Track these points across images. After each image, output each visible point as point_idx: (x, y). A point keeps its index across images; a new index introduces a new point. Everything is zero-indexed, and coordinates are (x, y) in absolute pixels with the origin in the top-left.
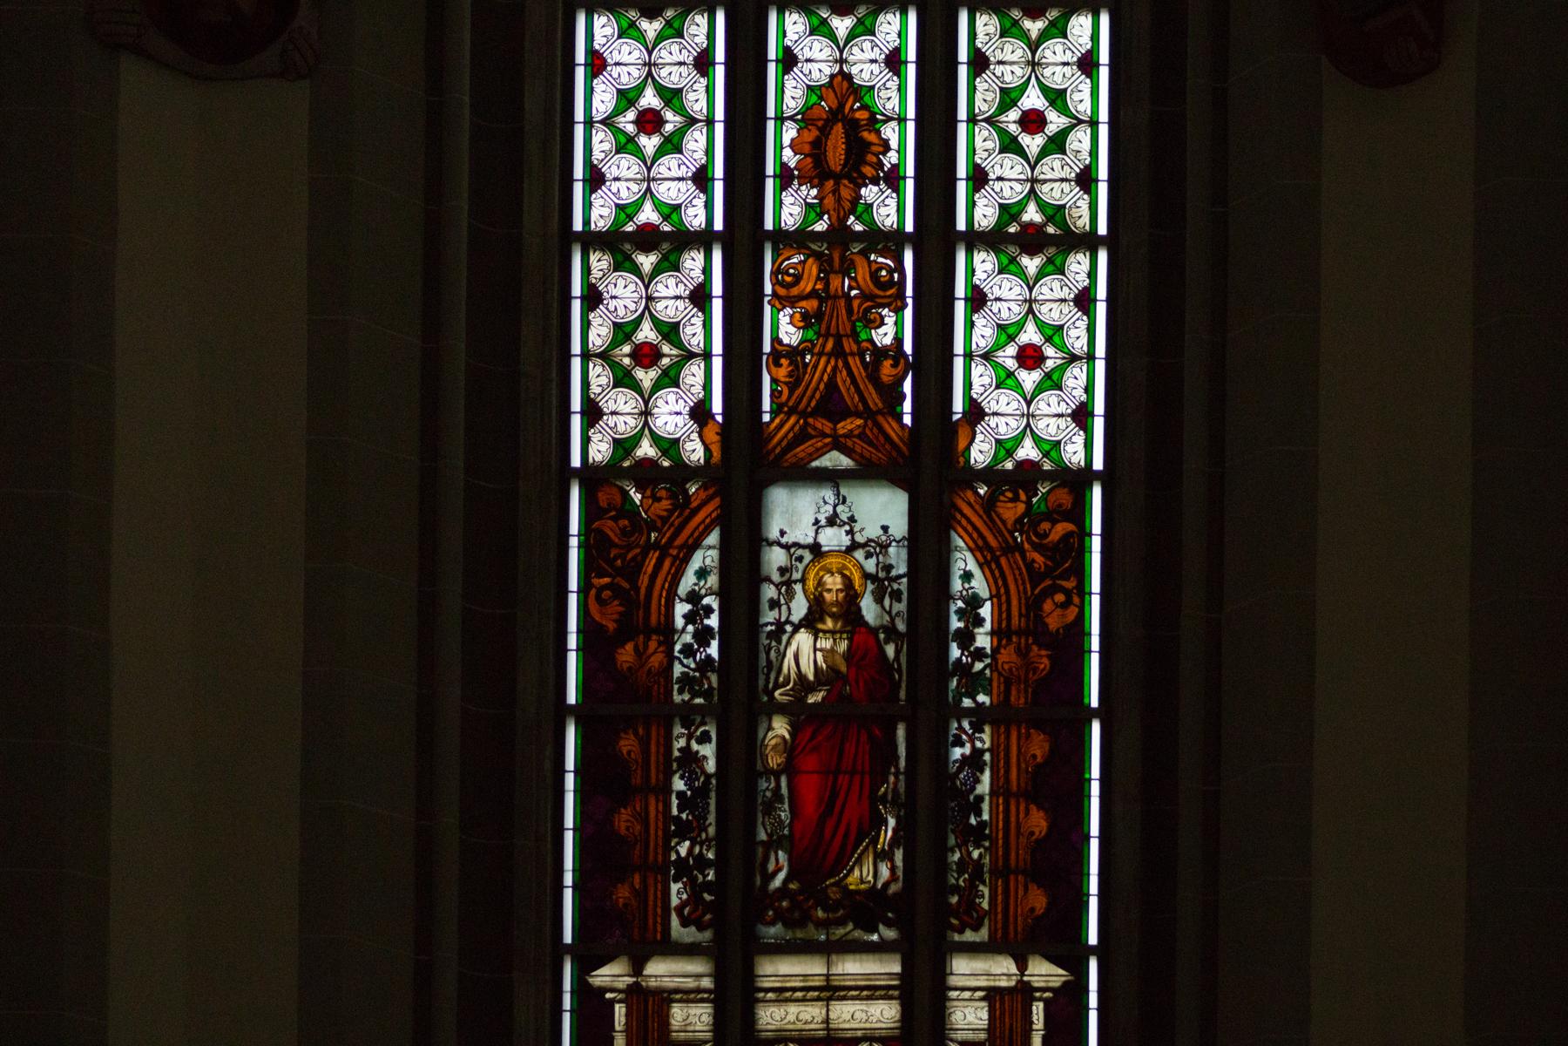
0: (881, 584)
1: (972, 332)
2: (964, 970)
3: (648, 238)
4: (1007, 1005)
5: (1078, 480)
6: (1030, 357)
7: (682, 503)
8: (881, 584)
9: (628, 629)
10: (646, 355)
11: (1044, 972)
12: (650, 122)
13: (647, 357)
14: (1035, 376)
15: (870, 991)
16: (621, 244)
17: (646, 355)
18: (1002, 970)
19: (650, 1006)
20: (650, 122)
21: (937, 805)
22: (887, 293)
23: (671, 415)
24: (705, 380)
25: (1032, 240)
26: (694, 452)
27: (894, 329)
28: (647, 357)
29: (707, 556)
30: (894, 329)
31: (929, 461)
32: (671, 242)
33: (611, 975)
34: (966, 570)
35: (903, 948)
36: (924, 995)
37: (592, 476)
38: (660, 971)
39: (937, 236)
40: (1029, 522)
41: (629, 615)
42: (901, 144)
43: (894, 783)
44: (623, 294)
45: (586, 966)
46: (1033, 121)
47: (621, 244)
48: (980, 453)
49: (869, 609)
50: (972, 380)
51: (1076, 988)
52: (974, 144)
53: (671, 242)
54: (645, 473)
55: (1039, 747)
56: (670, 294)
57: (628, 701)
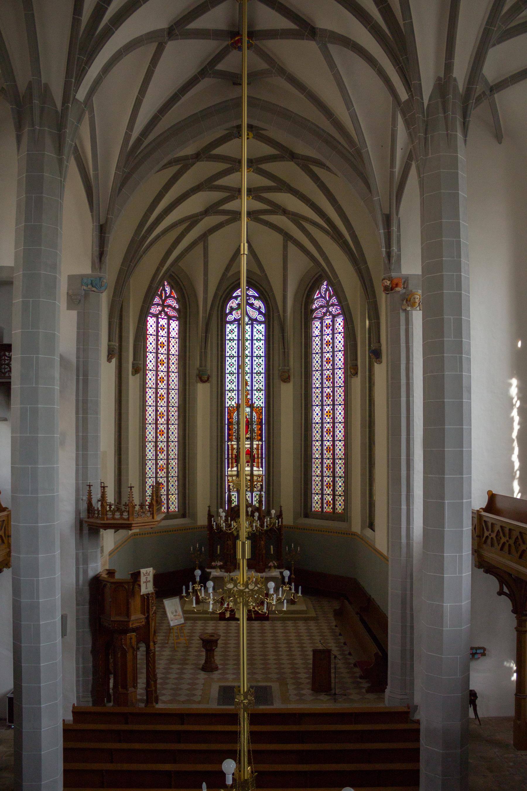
0: (248, 415)
1: (254, 397)
2: (254, 442)
3: (231, 390)
4: (258, 445)
5: (262, 407)
6: (259, 399)
7: (234, 409)
8: (248, 415)
9: (230, 418)
10: (231, 399)
11: (260, 443)
12: (231, 382)
13: (231, 399)
14: (259, 399)
15: (248, 444)
16: (229, 391)
17: (231, 399)
18: (257, 443)
19: (232, 445)
20: (231, 382)
21: (252, 431)
22: (248, 394)
23: (233, 403)
24: (236, 400)
25: (259, 390)
26: (235, 406)
27: (249, 397)
28: (231, 399)
29: (236, 413)
30: (249, 397)
31: (251, 406)
32: (233, 390)
33: (229, 443)
34: (254, 413)
35: (251, 441)
36: (252, 444)
37: (228, 407)
38: (233, 443)
39: (252, 390)
40: (259, 410)
41: (230, 418)
42: (249, 383)
43: (249, 429)
44: (230, 394)
45: (228, 442)
46: (259, 382)
47: (229, 391)
48: (255, 405)
49: (247, 417)
50: (254, 400)
51: (262, 444)
52: (254, 383)
53: (233, 390)
54: (231, 407)
55: (260, 427)
56: (233, 394)
57: (230, 423)
